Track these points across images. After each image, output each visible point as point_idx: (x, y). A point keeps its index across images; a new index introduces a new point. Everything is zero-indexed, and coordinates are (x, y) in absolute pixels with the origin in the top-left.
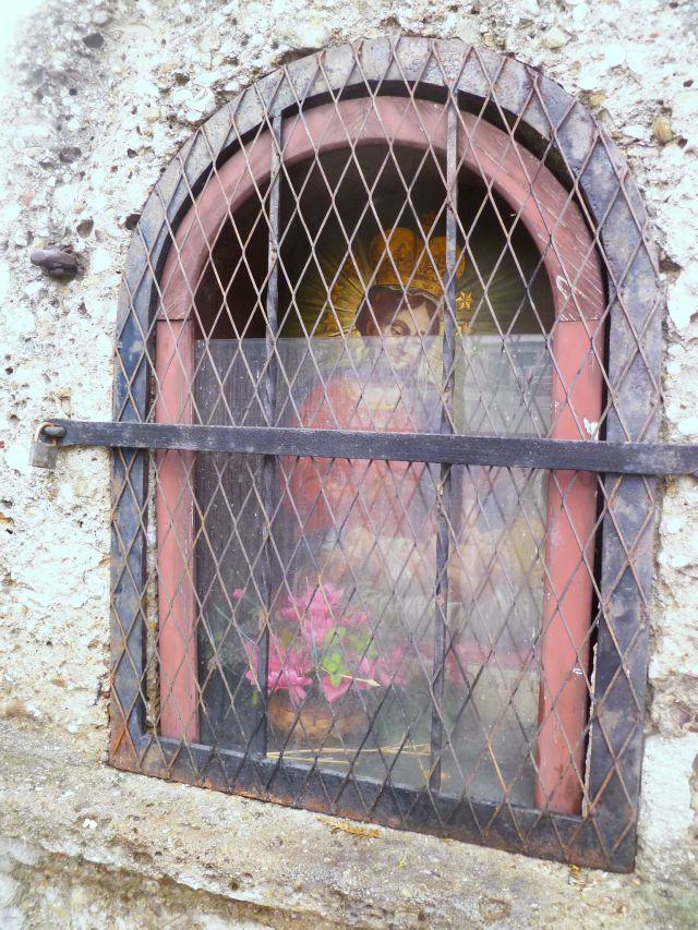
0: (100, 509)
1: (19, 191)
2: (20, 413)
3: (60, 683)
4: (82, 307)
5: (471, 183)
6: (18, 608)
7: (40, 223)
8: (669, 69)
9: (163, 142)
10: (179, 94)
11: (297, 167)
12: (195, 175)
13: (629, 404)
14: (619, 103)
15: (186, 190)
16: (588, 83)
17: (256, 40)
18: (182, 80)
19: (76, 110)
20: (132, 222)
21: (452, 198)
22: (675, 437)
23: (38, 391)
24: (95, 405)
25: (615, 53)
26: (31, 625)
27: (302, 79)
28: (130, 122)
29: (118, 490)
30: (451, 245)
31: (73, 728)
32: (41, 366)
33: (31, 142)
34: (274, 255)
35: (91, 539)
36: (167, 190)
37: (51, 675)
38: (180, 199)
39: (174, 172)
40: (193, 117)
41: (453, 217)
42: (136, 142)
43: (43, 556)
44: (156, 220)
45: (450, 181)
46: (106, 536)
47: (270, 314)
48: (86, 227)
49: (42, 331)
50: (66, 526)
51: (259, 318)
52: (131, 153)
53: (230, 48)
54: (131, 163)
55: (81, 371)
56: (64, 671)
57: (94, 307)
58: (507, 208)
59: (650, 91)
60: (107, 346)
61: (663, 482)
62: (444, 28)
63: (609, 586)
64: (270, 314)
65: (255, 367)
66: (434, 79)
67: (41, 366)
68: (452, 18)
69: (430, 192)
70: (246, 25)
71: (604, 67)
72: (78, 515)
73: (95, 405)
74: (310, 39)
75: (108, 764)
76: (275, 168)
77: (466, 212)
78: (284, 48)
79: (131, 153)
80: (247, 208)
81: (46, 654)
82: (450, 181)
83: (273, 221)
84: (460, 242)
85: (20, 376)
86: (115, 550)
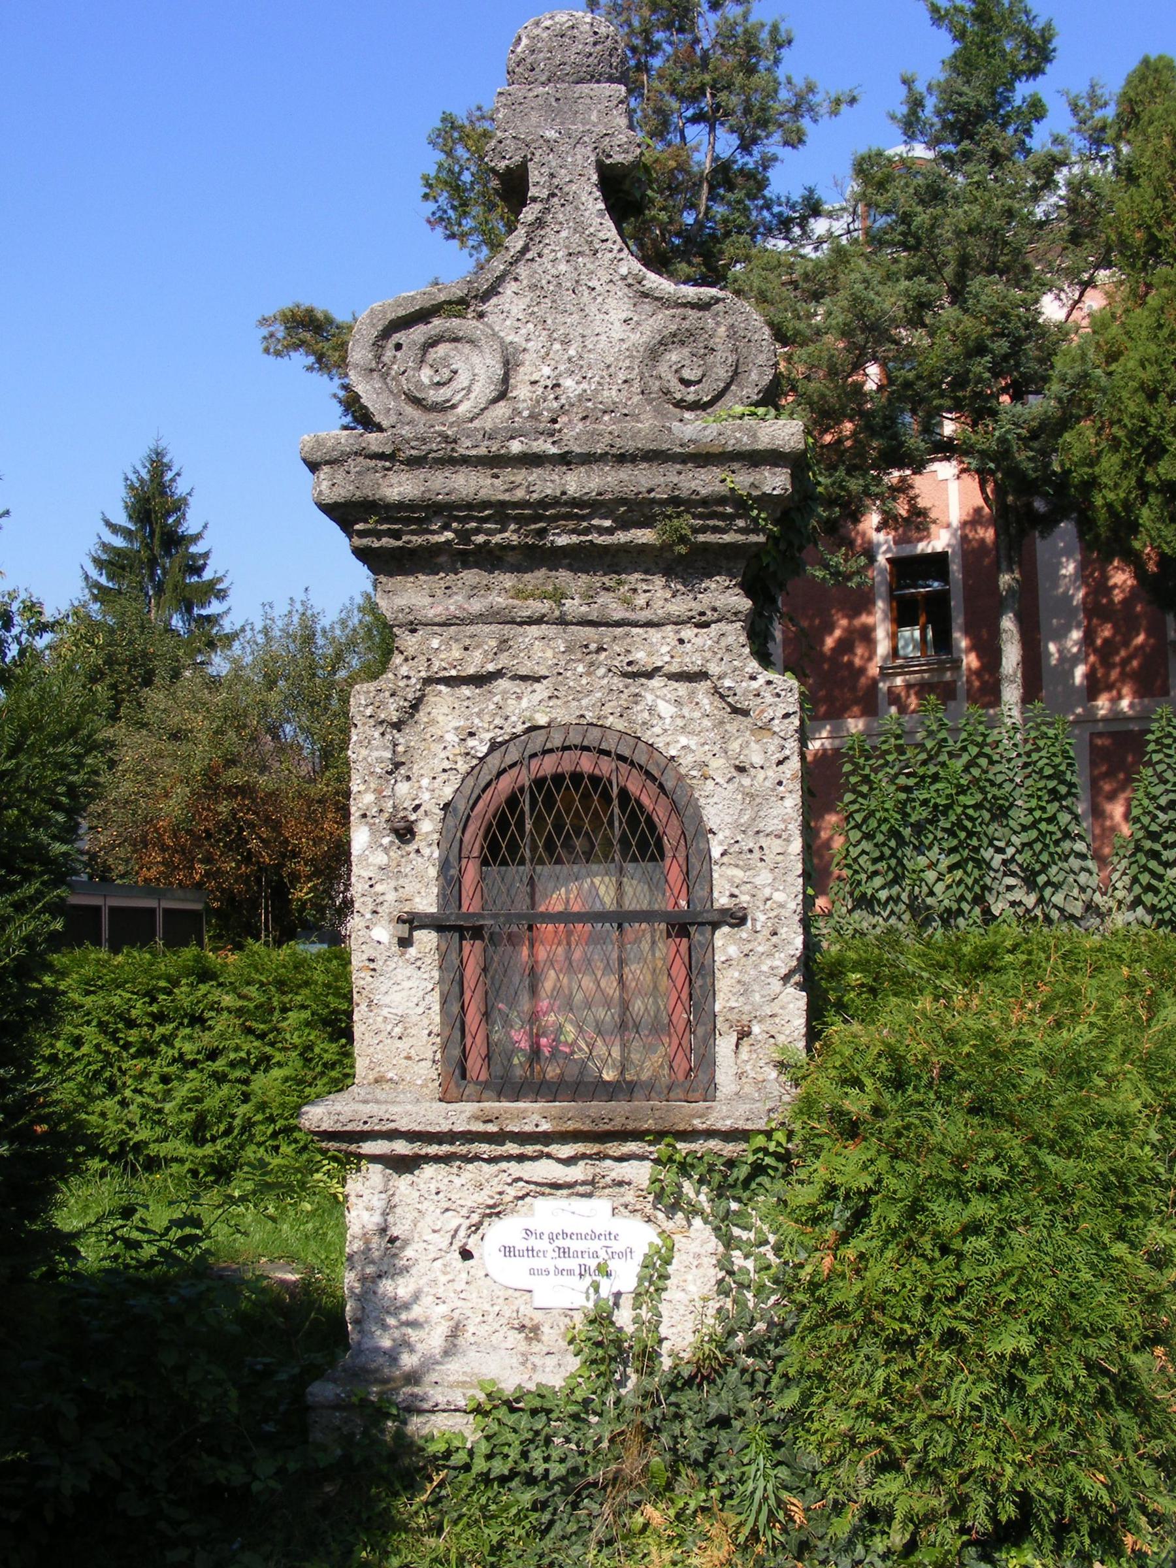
0: (432, 960)
1: (373, 786)
2: (379, 909)
3: (408, 1058)
4: (418, 851)
5: (624, 794)
6: (380, 1019)
7: (388, 805)
8: (707, 747)
9: (463, 767)
10: (471, 742)
11: (539, 782)
12: (483, 784)
13: (700, 892)
14: (687, 761)
15: (477, 792)
16: (673, 753)
17: (514, 718)
18: (472, 734)
19: (401, 740)
20: (446, 807)
21: (616, 802)
22: (716, 906)
23: (391, 897)
24: (427, 903)
25: (684, 741)
26: (389, 1028)
27: (537, 742)
28: (443, 755)
29: (443, 947)
30: (617, 824)
31: (419, 1082)
32: (393, 884)
33: (380, 760)
34: (528, 826)
35: (426, 976)
36: (467, 791)
37: (404, 1054)
38: (474, 796)
39: (470, 781)
40: (480, 755)
41: (617, 810)
42: (447, 765)
43: (396, 988)
44: (462, 806)
45: (615, 792)
46: (436, 974)
47: (528, 854)
48: (417, 808)
49: (394, 864)
50: (410, 970)
51: (523, 857)
52: (444, 771)
53: (498, 721)
54: (445, 776)
55: (419, 886)
56: (413, 1052)
57: (426, 851)
58: (641, 806)
59: (699, 757)
60: (433, 872)
61: (715, 926)
62: (608, 723)
63: (695, 972)
64: (528, 854)
65: (43, 883)
66: (604, 746)
67: (393, 884)
68: (611, 719)
69: (606, 798)
70: (508, 711)
71: (679, 746)
72: (419, 963)
73: (427, 903)
74: (542, 720)
75: (440, 1100)
76: (527, 784)
77: (623, 807)
78: (528, 725)
79: (444, 771)
80: (512, 801)
81: (399, 1044)
82: (615, 792)
83: (527, 808)
84: (621, 823)
85: (379, 888)
86: (441, 982)
